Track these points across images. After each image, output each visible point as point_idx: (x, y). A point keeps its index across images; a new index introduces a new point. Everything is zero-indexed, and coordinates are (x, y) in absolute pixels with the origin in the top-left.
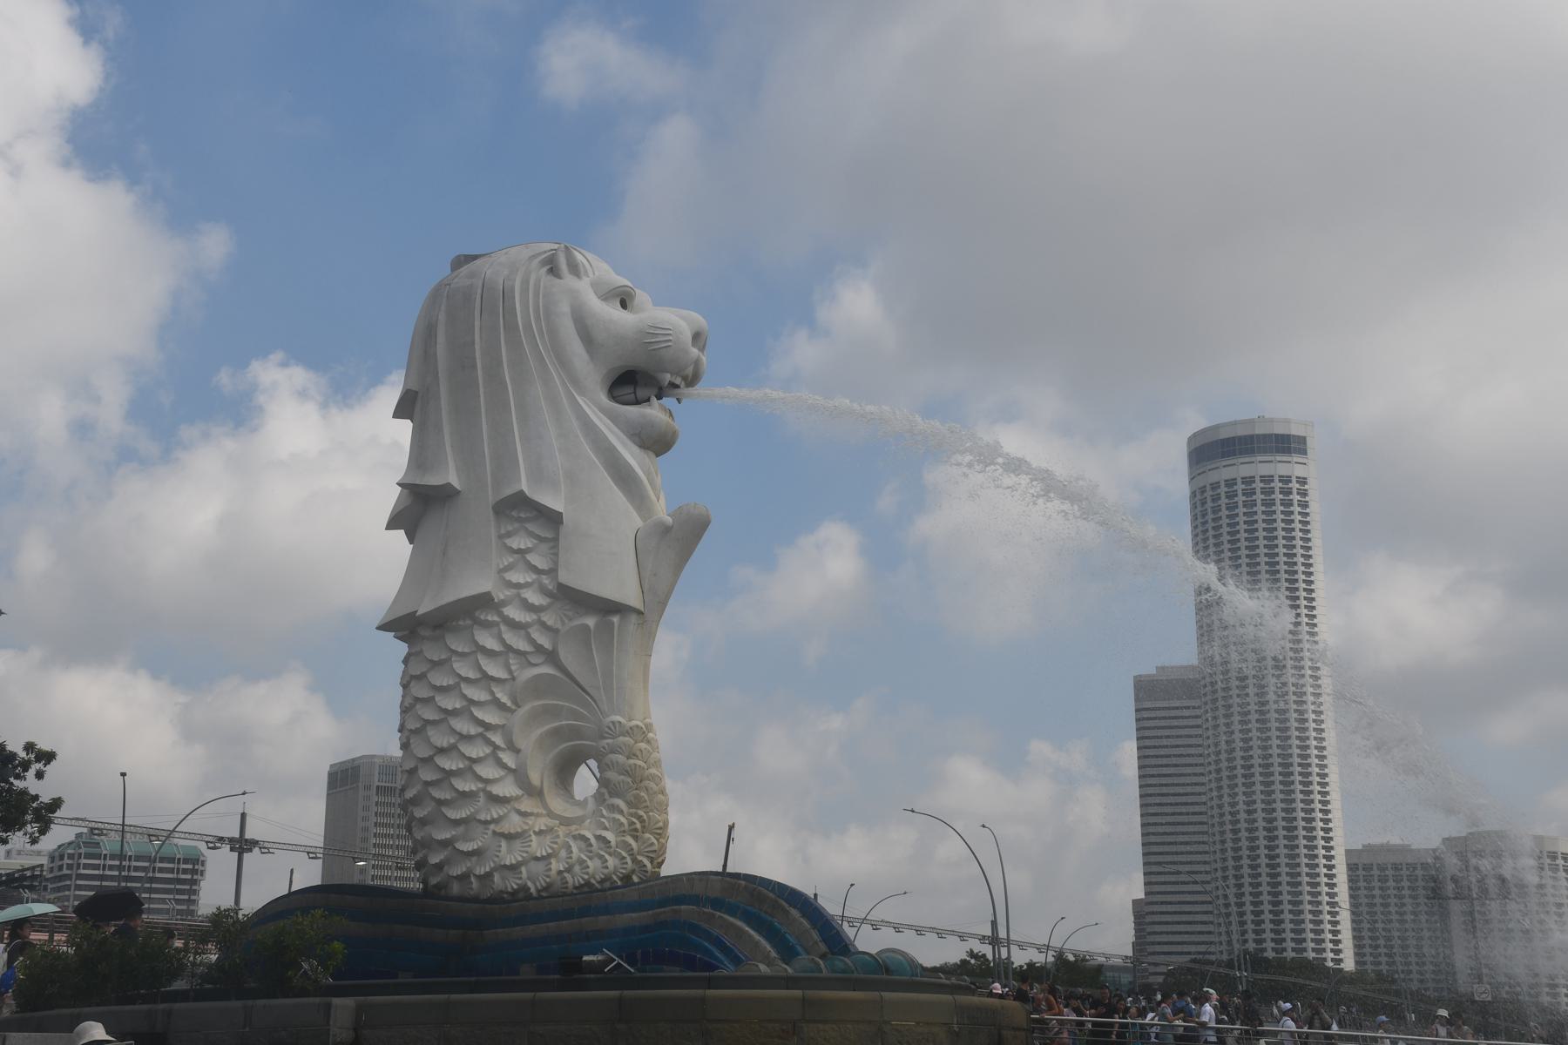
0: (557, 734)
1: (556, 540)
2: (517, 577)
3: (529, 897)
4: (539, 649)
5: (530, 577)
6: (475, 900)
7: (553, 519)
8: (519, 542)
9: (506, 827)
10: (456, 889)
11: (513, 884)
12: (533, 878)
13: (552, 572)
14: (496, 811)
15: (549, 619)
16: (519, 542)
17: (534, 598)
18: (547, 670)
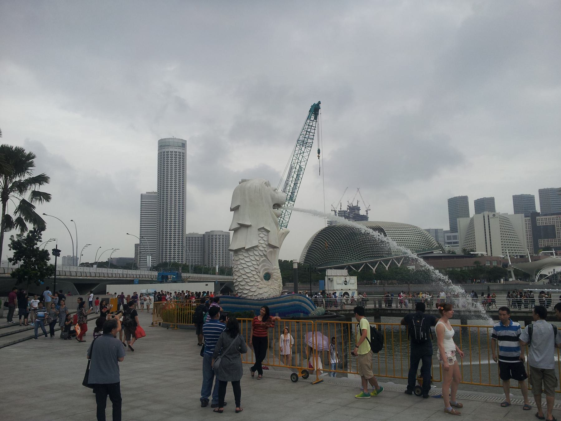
0: (265, 270)
1: (268, 235)
2: (262, 242)
3: (264, 300)
4: (264, 255)
5: (263, 242)
6: (254, 300)
7: (268, 231)
8: (262, 235)
9: (259, 287)
10: (249, 298)
11: (261, 297)
12: (265, 296)
13: (268, 241)
14: (257, 284)
15: (266, 249)
16: (262, 235)
17: (265, 246)
18: (264, 258)
